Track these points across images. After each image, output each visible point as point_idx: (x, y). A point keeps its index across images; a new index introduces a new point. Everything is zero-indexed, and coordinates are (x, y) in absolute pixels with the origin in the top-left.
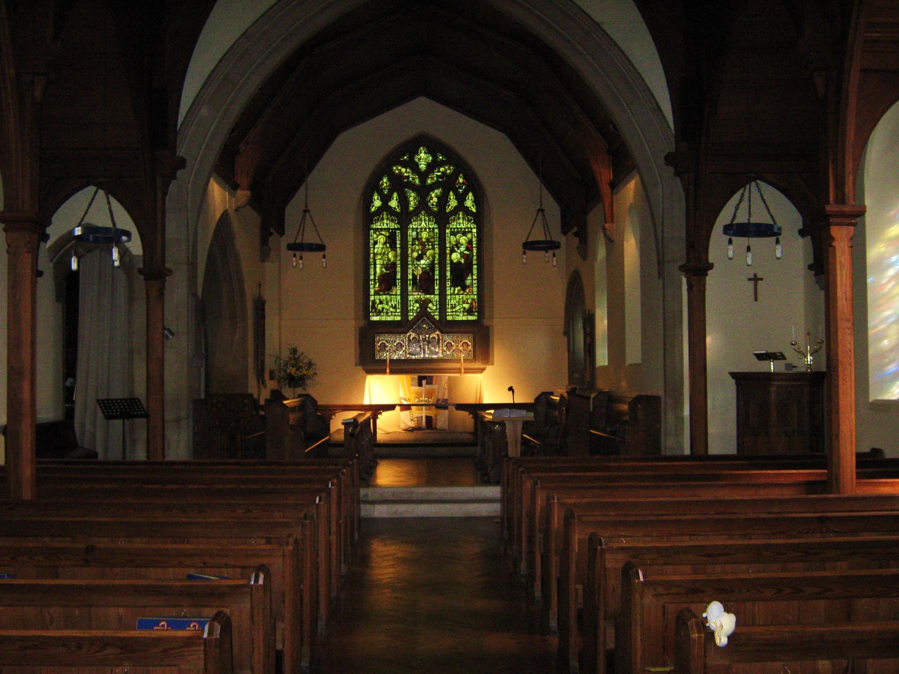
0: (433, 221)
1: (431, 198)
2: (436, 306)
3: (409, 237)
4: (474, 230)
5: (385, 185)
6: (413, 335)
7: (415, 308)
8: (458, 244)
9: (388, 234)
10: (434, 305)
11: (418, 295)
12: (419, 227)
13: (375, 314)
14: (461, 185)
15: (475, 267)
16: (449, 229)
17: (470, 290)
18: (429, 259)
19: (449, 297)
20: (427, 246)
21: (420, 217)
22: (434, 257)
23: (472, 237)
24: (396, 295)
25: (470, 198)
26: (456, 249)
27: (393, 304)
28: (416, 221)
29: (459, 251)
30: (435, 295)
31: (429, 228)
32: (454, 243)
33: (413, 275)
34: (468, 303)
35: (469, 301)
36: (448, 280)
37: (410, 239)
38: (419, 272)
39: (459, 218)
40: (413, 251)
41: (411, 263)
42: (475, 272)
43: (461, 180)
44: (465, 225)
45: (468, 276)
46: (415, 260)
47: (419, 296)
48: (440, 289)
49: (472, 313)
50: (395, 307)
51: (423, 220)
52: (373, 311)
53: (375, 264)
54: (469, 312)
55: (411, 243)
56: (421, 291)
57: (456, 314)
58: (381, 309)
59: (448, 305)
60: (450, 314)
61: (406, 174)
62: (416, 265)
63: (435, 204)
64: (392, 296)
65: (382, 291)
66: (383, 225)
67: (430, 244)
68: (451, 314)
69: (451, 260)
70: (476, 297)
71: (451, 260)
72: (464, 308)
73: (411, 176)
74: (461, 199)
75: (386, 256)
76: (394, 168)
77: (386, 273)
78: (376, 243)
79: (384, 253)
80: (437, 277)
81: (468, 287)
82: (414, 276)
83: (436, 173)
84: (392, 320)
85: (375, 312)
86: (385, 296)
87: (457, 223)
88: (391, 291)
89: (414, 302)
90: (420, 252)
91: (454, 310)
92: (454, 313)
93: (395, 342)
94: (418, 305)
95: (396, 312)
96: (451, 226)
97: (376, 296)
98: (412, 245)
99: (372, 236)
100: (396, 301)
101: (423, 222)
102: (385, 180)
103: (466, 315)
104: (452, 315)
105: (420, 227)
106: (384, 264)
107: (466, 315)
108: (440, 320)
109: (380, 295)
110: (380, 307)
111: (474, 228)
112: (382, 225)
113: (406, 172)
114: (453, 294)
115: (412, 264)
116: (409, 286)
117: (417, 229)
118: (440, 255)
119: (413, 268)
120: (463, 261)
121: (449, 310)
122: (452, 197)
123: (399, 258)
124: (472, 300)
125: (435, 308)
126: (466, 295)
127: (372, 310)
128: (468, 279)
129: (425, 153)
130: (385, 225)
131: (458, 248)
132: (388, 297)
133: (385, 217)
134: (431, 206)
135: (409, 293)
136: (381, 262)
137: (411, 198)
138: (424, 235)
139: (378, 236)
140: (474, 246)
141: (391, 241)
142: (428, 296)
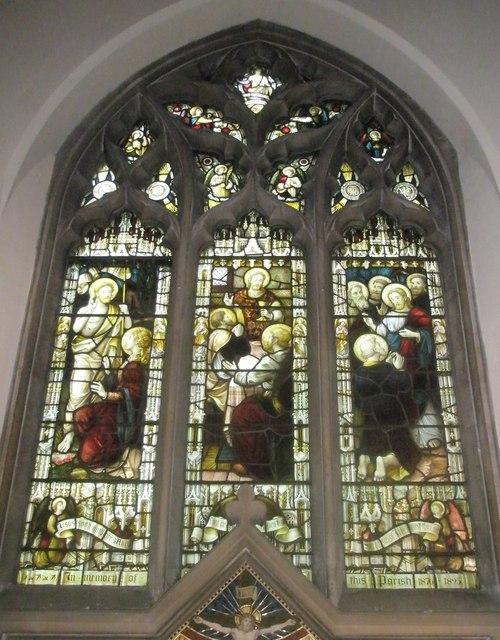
0: (285, 239)
1: (282, 179)
3: (199, 283)
5: (136, 144)
7: (212, 537)
8: (376, 309)
9: (129, 276)
10: (291, 526)
11: (226, 482)
12: (235, 255)
13: (40, 558)
14: (377, 146)
16: (344, 263)
17: (433, 465)
18: (269, 352)
19: (351, 494)
20: (264, 313)
22: (289, 349)
23: (427, 286)
24: (136, 481)
26: (369, 322)
27: (122, 516)
28: (227, 238)
29: (381, 329)
30: (295, 483)
31: (274, 259)
32: (362, 304)
33: (210, 408)
34: (431, 518)
35: (437, 510)
36: (346, 426)
37: (204, 290)
38: (231, 398)
39: (375, 233)
41: (203, 366)
42: (447, 398)
44: (396, 250)
45: (422, 412)
46: (220, 358)
47: (227, 489)
49: (456, 564)
50: (127, 533)
51: (253, 235)
52: (35, 544)
53: (69, 368)
54: (441, 555)
55: (207, 301)
56: (239, 466)
57: (384, 565)
58: (68, 535)
59: (351, 524)
60: (357, 562)
61: (203, 120)
62: (221, 374)
63: (292, 192)
64: (120, 487)
65: (82, 465)
66: (115, 249)
67: (276, 304)
70: (461, 493)
71: (355, 363)
72: (419, 538)
73: (216, 124)
74: (378, 183)
75: (114, 344)
77: (107, 404)
78: (82, 300)
79: (107, 334)
80: (300, 416)
81: (428, 453)
82: (213, 415)
83: (296, 119)
84: (109, 583)
85: (44, 549)
87: (369, 246)
89: (206, 510)
90: (238, 331)
91: (376, 546)
92: (378, 560)
94: (221, 524)
95: (129, 551)
97: (54, 485)
98: (212, 307)
100: (135, 506)
104: (370, 568)
105: (242, 254)
107: (427, 570)
108: (319, 583)
109: (71, 480)
110: (65, 528)
111: (429, 259)
112: (111, 247)
114: (368, 481)
117: (229, 259)
118: (310, 340)
119: (210, 385)
120: (398, 362)
121: (356, 547)
122: (348, 177)
123: (160, 349)
124: (446, 503)
125: (293, 535)
126: (420, 484)
127: (30, 541)
130: (122, 247)
131: (378, 320)
132: (105, 489)
134: (279, 198)
139: (93, 280)
140: (434, 312)
141: (138, 297)
142: (266, 488)
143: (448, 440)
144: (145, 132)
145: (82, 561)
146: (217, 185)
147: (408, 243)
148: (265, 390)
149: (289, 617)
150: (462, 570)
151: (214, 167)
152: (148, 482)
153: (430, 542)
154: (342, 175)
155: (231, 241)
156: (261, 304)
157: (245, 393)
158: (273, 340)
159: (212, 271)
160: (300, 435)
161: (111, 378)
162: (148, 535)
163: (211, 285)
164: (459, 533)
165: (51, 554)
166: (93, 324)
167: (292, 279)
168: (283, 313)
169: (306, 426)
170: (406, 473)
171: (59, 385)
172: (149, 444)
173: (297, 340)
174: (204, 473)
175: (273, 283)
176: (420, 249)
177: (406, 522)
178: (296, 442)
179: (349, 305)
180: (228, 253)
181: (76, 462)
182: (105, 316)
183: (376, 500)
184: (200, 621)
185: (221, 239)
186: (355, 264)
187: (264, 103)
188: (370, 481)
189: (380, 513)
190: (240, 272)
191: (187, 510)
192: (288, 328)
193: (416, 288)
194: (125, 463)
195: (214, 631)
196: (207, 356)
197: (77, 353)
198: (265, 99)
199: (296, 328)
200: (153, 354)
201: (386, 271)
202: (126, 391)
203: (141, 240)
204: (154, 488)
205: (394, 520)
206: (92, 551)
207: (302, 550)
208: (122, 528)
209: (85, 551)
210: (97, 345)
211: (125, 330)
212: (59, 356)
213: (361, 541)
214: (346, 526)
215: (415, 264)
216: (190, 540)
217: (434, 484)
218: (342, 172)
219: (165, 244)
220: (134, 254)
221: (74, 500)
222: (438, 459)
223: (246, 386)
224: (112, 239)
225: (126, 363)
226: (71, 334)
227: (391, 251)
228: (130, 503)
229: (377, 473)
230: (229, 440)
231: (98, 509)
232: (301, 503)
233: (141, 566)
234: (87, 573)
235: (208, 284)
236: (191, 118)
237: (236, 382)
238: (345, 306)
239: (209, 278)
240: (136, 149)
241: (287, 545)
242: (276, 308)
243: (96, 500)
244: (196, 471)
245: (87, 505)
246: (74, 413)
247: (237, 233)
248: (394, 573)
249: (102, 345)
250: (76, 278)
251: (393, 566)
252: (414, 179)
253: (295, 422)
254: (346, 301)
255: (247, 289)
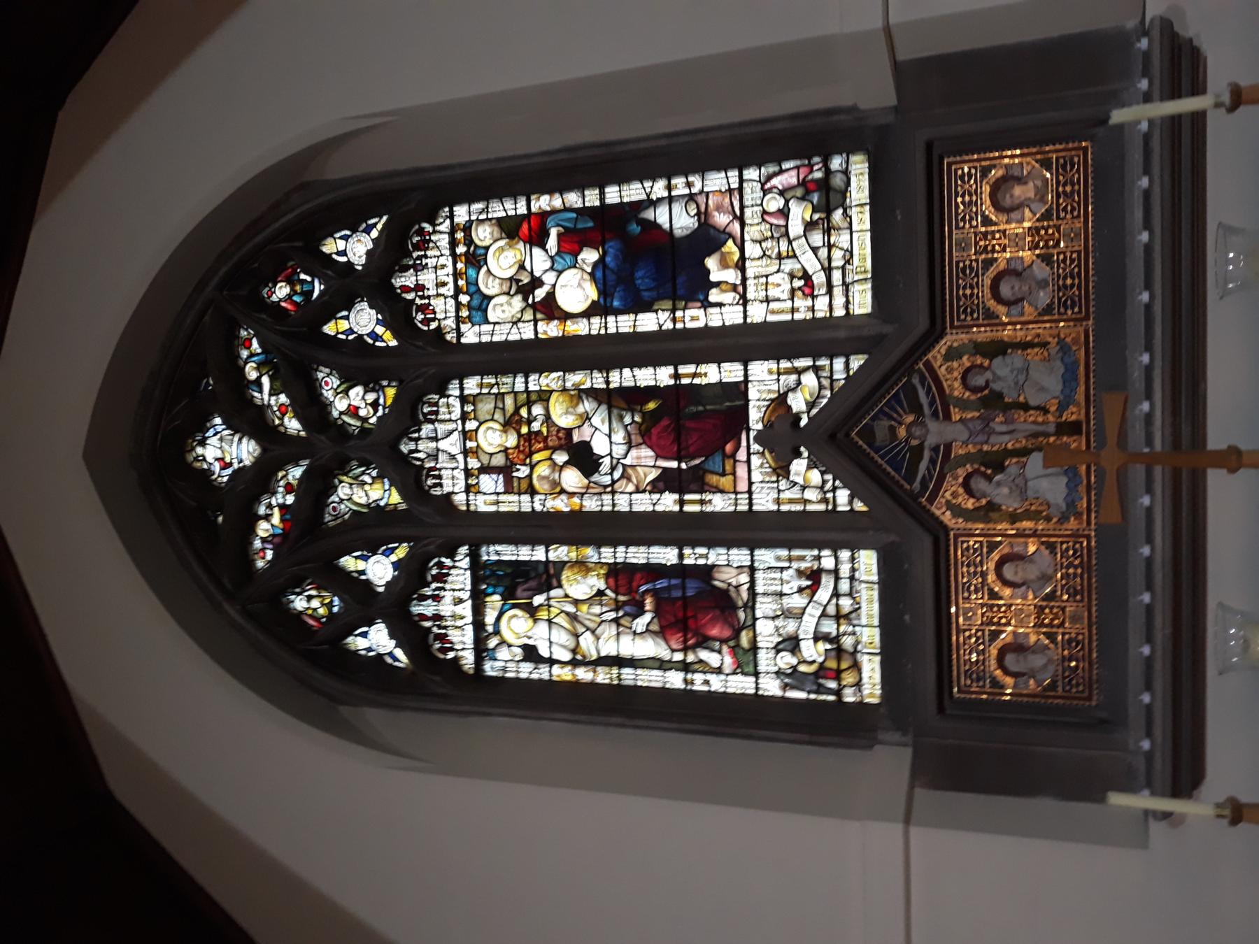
0: (436, 404)
1: (353, 411)
2: (799, 372)
4: (461, 213)
5: (315, 603)
6: (952, 489)
7: (815, 477)
8: (525, 286)
9: (497, 597)
10: (799, 383)
11: (748, 462)
12: (462, 466)
13: (849, 678)
14: (298, 288)
15: (613, 195)
16: (464, 328)
17: (719, 208)
18: (587, 418)
19: (757, 313)
20: (536, 426)
21: (422, 460)
22: (581, 393)
23: (488, 219)
24: (752, 570)
25: (341, 245)
26: (540, 294)
28: (440, 477)
29: (549, 278)
30: (746, 381)
31: (464, 417)
32: (517, 302)
34: (784, 213)
35: (774, 203)
36: (674, 320)
37: (513, 503)
39: (420, 287)
40: (558, 490)
41: (607, 498)
42: (634, 192)
43: (282, 291)
44: (442, 261)
45: (654, 225)
46: (595, 478)
47: (756, 461)
48: (719, 358)
49: (838, 181)
50: (815, 577)
51: (434, 445)
53: (618, 662)
55: (526, 498)
56: (729, 447)
57: (843, 268)
58: (822, 646)
60: (839, 300)
61: (276, 519)
62: (617, 475)
63: (371, 397)
64: (760, 589)
65: (736, 635)
66: (462, 618)
67: (524, 412)
68: (838, 292)
69: (587, 314)
70: (751, 174)
71: (591, 312)
72: (809, 226)
73: (281, 501)
75: (584, 608)
76: (260, 564)
77: (658, 612)
78: (530, 653)
79: (573, 618)
80: (663, 376)
81: (703, 216)
82: (664, 482)
83: (266, 397)
84: (876, 594)
85: (837, 675)
86: (759, 624)
87: (438, 295)
88: (733, 593)
89: (783, 484)
90: (561, 458)
91: (819, 278)
92: (837, 276)
93: (994, 595)
94: (798, 466)
95: (836, 572)
96: (450, 323)
97: (762, 668)
98: (532, 492)
99: (505, 670)
100: (782, 569)
101: (442, 445)
102: (299, 603)
103: (845, 214)
104: (846, 286)
105: (460, 458)
106: (616, 621)
109: (754, 648)
111: (451, 217)
112: (459, 623)
113: (267, 517)
115: (613, 492)
116: (708, 508)
117: (468, 473)
118: (569, 367)
119: (631, 488)
120: (590, 256)
121: (822, 304)
122: (344, 325)
123: (590, 552)
124: (765, 192)
125: (809, 380)
126: (743, 225)
128: (667, 226)
129: (203, 443)
130: (459, 609)
131: (536, 282)
132: (764, 607)
133: (427, 608)
134: (380, 413)
135: (743, 507)
136: (609, 631)
137: (355, 498)
138: (493, 439)
139: (503, 642)
140: (522, 210)
143: (686, 191)
144: (299, 594)
145: (850, 629)
146: (367, 495)
147: (431, 245)
148: (633, 421)
149: (909, 381)
150: (846, 173)
151: (342, 500)
152: (752, 556)
153: (814, 210)
154: (342, 333)
155: (443, 472)
156: (524, 430)
157: (638, 445)
158: (571, 414)
159: (485, 494)
160: (687, 376)
161: (628, 609)
162: (816, 552)
163: (504, 493)
164: (801, 177)
165: (844, 665)
166: (561, 637)
167: (489, 393)
168: (535, 402)
169: (676, 370)
170: (730, 243)
171: (639, 671)
172: (706, 557)
173: (569, 385)
174: (739, 489)
175: (496, 417)
176: (438, 228)
177: (790, 242)
178: (697, 381)
179: (519, 320)
180: (460, 475)
181: (732, 643)
182: (550, 621)
183: (764, 280)
184: (917, 485)
185: (441, 485)
186: (464, 313)
187: (245, 440)
188: (740, 289)
189: (780, 275)
190: (485, 459)
191: (784, 508)
192: (555, 395)
193: (492, 234)
194: (729, 584)
195: (928, 469)
196: (595, 494)
197: (598, 652)
198: (240, 440)
199: (554, 386)
200: (595, 559)
201: (472, 272)
202: (643, 588)
203: (448, 586)
204: (760, 547)
205: (788, 257)
206: (838, 617)
207: (828, 368)
208: (809, 583)
209: (839, 625)
210: (588, 629)
211: (567, 596)
212: (603, 676)
213: (814, 297)
214: (798, 316)
215: (460, 235)
216: (820, 502)
217: (742, 208)
218: (338, 333)
219: (452, 555)
220: (468, 594)
221: (779, 643)
222: (710, 202)
223: (630, 445)
224: (448, 623)
225: (608, 592)
226: (574, 663)
227: (443, 266)
228: (778, 575)
229: (731, 281)
230: (697, 462)
231: (787, 614)
232: (770, 372)
233: (853, 559)
234: (864, 621)
235: (502, 498)
236: (274, 536)
237: (625, 456)
238: (520, 325)
239: (494, 497)
240: (323, 604)
241: (821, 387)
242: (529, 412)
243: (778, 616)
244: (736, 499)
245: (784, 627)
246: (673, 651)
247: (432, 464)
248: (852, 256)
249: (587, 623)
250: (502, 664)
251: (844, 256)
252: (341, 238)
253: (672, 382)
254: (515, 323)
255: (507, 449)
